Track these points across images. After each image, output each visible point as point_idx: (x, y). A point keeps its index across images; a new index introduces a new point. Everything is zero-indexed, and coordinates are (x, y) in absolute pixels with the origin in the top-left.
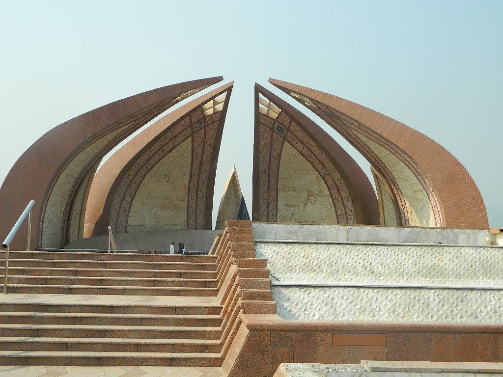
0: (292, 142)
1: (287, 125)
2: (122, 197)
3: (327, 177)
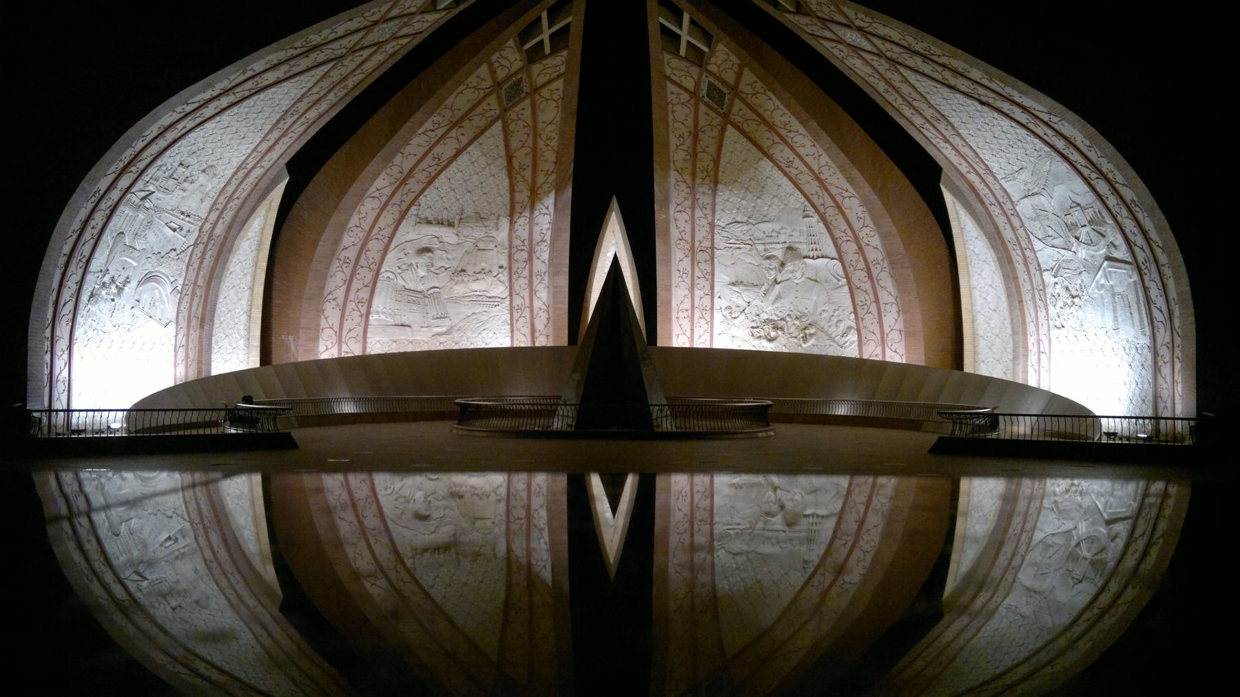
0: (747, 129)
1: (730, 77)
2: (348, 271)
3: (831, 212)
